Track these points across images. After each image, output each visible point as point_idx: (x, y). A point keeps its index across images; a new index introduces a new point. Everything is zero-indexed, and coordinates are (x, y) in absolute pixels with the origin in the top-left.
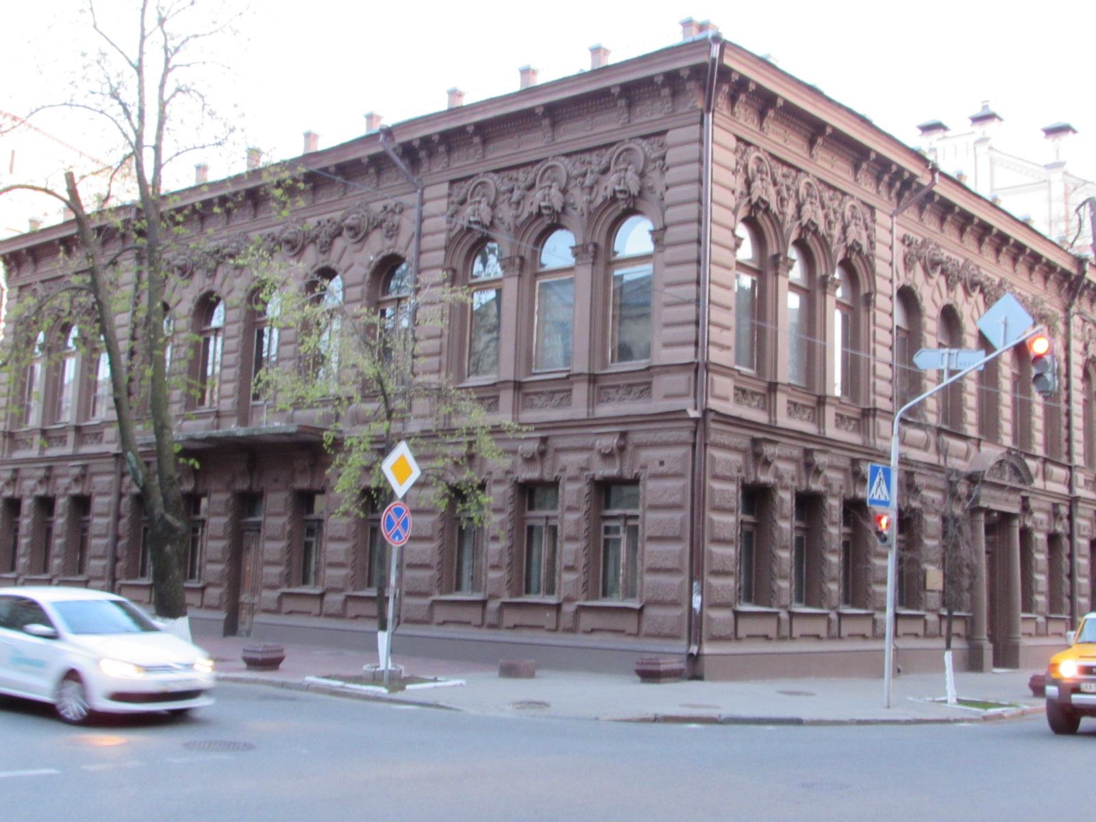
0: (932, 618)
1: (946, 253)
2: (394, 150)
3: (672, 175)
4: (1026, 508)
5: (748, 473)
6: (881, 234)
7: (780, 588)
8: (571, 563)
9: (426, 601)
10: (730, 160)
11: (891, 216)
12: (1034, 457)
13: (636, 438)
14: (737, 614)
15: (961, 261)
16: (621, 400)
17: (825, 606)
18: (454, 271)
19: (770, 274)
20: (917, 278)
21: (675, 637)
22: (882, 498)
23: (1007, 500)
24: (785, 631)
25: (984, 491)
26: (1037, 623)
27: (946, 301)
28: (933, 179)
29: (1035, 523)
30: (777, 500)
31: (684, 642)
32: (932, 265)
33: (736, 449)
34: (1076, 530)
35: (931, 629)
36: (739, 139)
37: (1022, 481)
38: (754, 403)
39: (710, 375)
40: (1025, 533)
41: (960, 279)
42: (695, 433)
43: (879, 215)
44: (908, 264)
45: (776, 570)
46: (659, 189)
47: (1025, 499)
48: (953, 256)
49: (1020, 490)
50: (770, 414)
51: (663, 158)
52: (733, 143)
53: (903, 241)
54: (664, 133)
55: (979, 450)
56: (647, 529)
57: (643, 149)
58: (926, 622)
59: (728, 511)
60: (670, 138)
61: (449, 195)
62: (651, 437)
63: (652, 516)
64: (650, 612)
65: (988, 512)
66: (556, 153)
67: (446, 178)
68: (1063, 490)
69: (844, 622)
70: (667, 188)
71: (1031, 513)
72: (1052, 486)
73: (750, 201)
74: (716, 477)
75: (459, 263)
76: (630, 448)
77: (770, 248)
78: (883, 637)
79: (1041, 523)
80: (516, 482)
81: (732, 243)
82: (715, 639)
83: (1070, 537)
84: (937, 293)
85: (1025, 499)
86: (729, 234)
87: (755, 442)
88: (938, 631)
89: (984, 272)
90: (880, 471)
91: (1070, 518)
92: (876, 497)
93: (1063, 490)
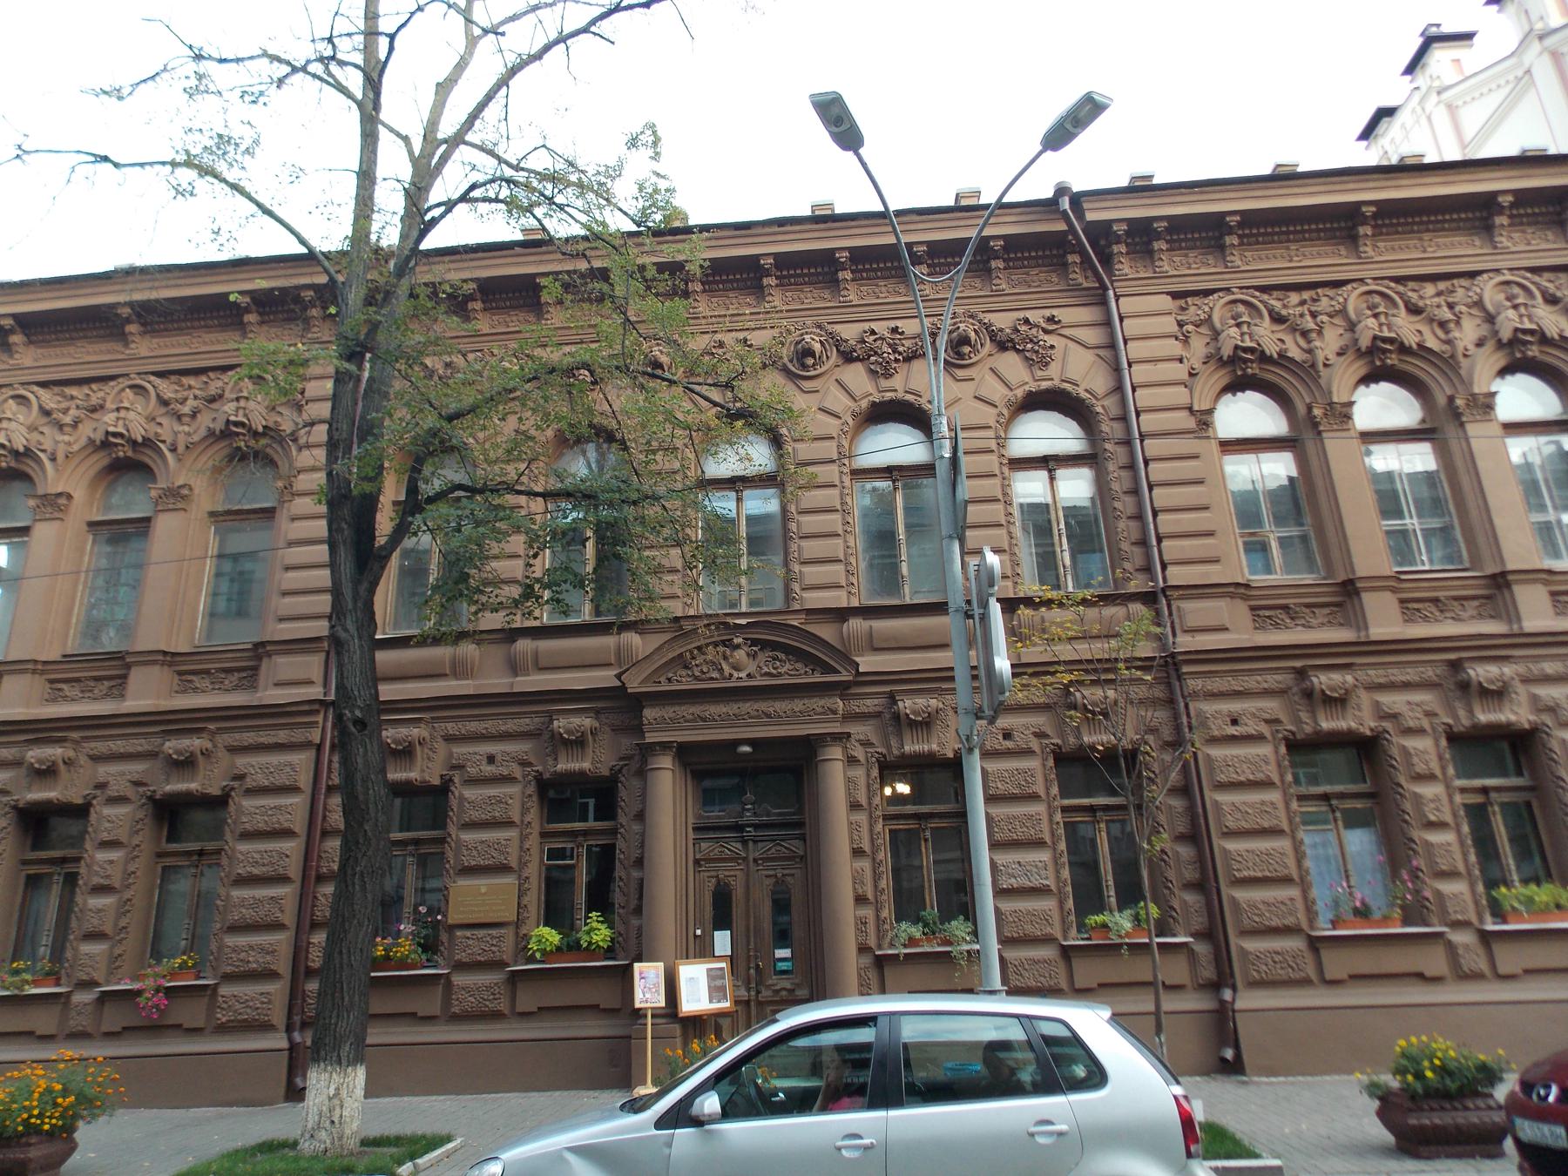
0: (1461, 938)
30: (1395, 752)
56: (87, 876)
65: (685, 753)
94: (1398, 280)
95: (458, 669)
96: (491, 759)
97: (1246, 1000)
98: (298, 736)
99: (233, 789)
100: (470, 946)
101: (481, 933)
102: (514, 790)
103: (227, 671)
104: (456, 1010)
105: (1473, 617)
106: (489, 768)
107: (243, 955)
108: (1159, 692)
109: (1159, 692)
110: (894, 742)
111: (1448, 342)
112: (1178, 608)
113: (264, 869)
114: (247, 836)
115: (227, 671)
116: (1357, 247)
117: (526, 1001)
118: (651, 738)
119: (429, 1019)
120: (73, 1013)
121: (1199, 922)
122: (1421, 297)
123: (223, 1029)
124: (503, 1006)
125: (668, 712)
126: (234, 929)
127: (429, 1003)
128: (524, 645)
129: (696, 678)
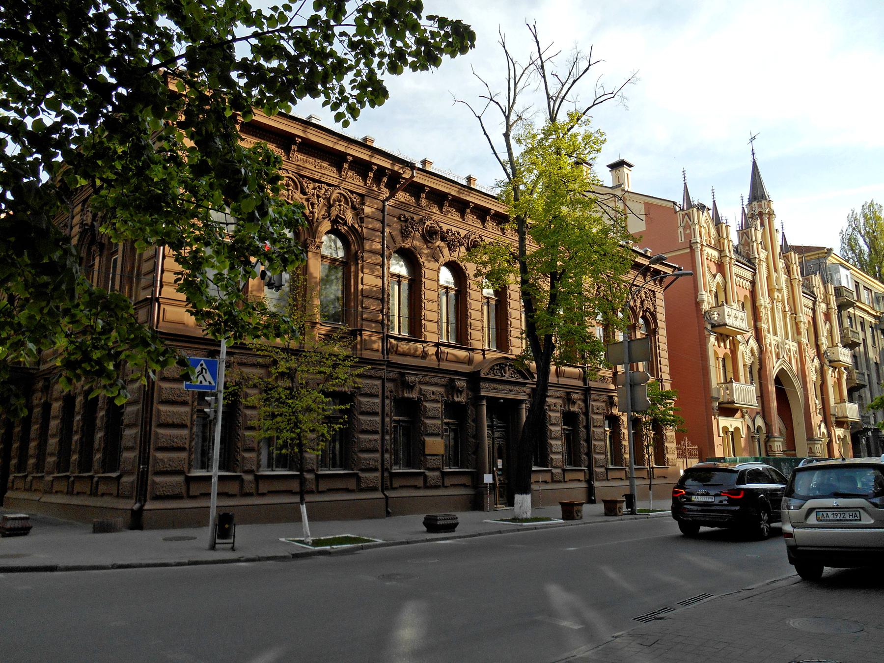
7: (244, 458)
14: (189, 480)
17: (238, 470)
21: (128, 497)
22: (204, 383)
26: (552, 473)
28: (413, 173)
31: (133, 501)
34: (590, 409)
35: (431, 482)
37: (525, 378)
45: (239, 445)
48: (454, 229)
49: (524, 384)
53: (399, 218)
58: (425, 477)
65: (490, 400)
67: (81, 200)
68: (580, 383)
82: (157, 498)
83: (586, 414)
88: (440, 483)
90: (202, 362)
91: (585, 401)
93: (580, 383)
96: (433, 393)
97: (597, 484)
98: (378, 374)
99: (355, 392)
100: (432, 462)
101: (434, 458)
102: (439, 405)
104: (428, 484)
106: (433, 396)
107: (368, 462)
108: (582, 397)
109: (582, 397)
113: (373, 428)
114: (363, 413)
117: (447, 482)
118: (483, 394)
119: (419, 488)
121: (586, 464)
123: (362, 490)
124: (440, 483)
125: (487, 385)
126: (362, 451)
127: (420, 482)
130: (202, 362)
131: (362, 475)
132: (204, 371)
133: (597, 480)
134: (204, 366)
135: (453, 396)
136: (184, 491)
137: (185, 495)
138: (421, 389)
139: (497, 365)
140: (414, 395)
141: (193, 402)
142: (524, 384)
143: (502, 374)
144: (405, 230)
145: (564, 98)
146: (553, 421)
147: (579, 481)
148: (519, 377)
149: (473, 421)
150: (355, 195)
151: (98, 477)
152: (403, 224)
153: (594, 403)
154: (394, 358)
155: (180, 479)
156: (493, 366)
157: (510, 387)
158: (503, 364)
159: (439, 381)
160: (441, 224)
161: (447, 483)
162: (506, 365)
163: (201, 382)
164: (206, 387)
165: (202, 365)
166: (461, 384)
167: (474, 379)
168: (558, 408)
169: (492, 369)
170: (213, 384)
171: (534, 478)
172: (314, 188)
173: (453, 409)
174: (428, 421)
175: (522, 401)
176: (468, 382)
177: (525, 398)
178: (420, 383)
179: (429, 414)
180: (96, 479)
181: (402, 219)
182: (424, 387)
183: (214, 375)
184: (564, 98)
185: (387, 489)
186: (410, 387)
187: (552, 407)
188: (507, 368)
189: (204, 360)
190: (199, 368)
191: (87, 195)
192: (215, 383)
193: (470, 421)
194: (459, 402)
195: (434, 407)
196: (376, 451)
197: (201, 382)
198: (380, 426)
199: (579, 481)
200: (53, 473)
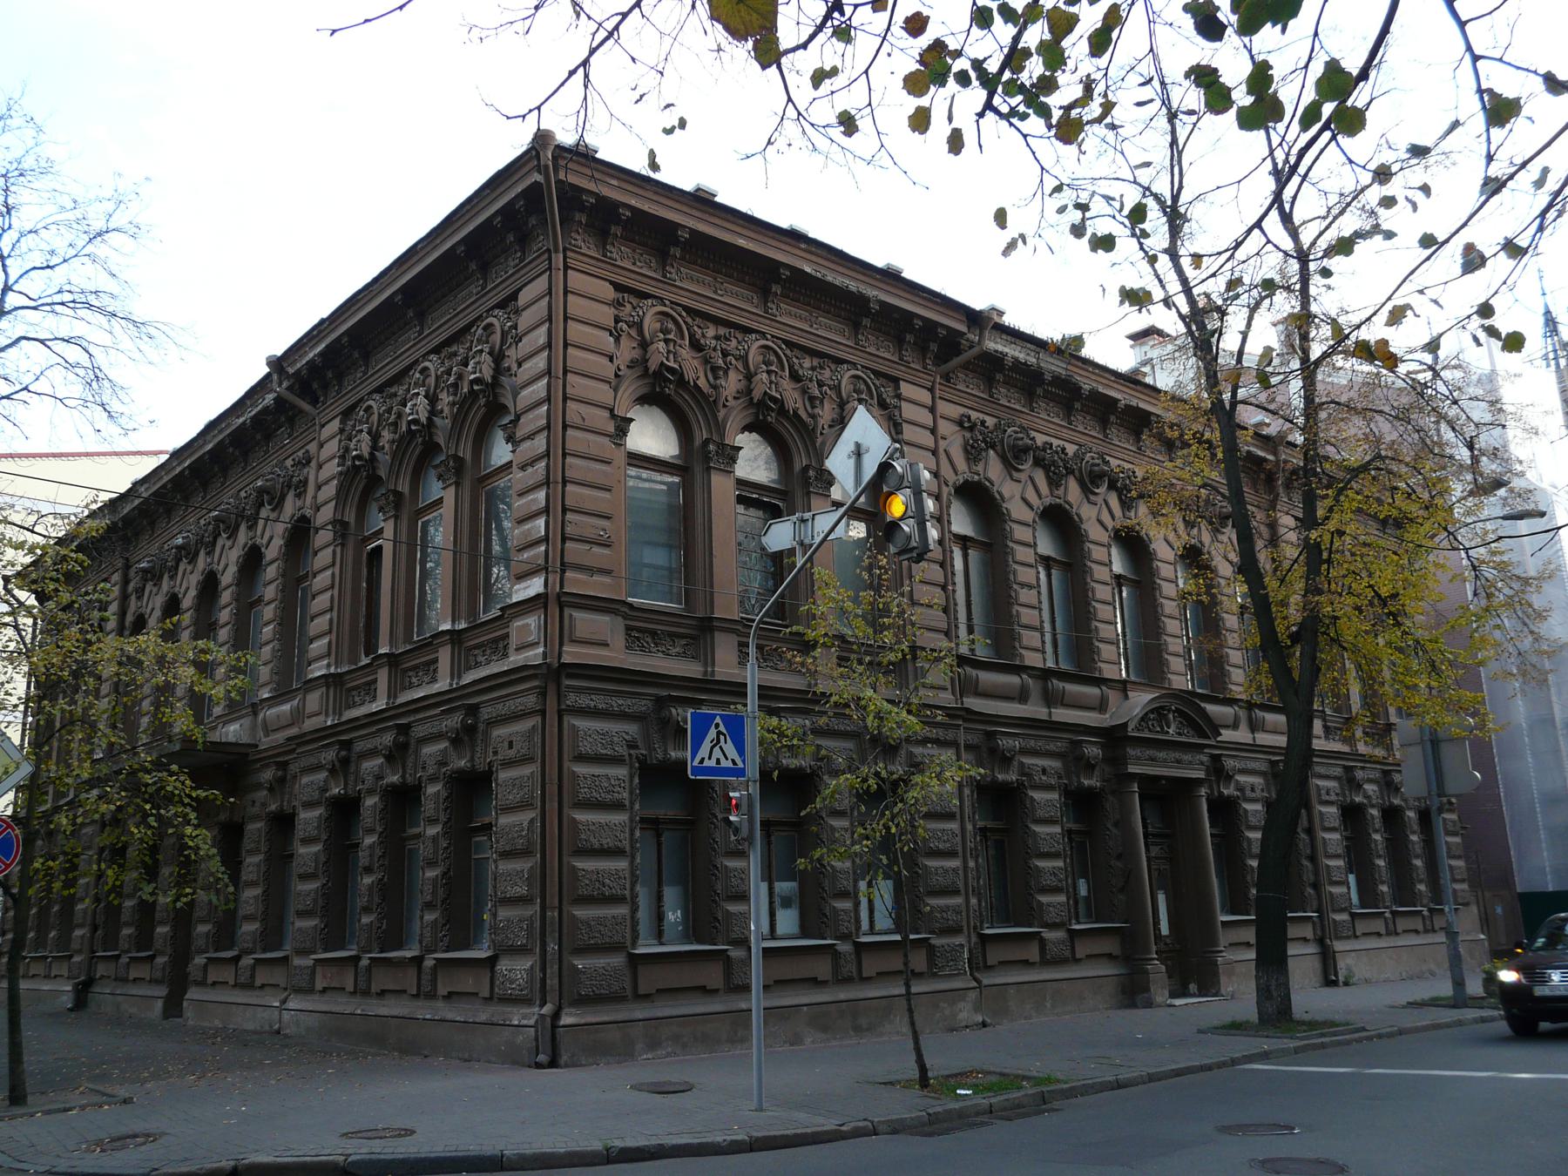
1: (1040, 439)
2: (289, 389)
3: (526, 345)
4: (1218, 771)
5: (651, 749)
6: (908, 411)
8: (429, 898)
9: (307, 962)
10: (606, 315)
11: (931, 390)
12: (1231, 702)
13: (486, 713)
14: (635, 961)
15: (1071, 449)
16: (488, 662)
18: (345, 525)
19: (698, 469)
20: (993, 469)
22: (725, 764)
23: (1178, 762)
24: (850, 968)
25: (1131, 752)
27: (1048, 501)
29: (1241, 789)
32: (1013, 457)
33: (622, 716)
36: (618, 287)
38: (674, 651)
39: (567, 611)
40: (1225, 810)
41: (1070, 472)
42: (543, 694)
43: (906, 389)
44: (973, 453)
45: (719, 888)
46: (514, 367)
47: (1216, 759)
48: (1055, 442)
50: (706, 665)
51: (515, 327)
52: (609, 293)
53: (960, 424)
54: (514, 296)
55: (1126, 697)
57: (497, 320)
58: (1043, 943)
59: (617, 806)
60: (524, 297)
61: (342, 431)
62: (503, 709)
63: (504, 820)
64: (503, 965)
65: (1144, 780)
66: (423, 351)
67: (339, 410)
69: (642, 970)
70: (520, 365)
71: (1229, 778)
72: (1263, 739)
73: (647, 369)
74: (581, 758)
75: (350, 517)
76: (481, 727)
77: (697, 433)
78: (746, 988)
79: (1253, 790)
80: (385, 790)
81: (611, 428)
84: (1030, 489)
85: (1216, 759)
86: (607, 414)
87: (661, 702)
88: (1068, 954)
89: (1114, 462)
90: (718, 720)
92: (707, 763)
94: (790, 344)
95: (1022, 696)
96: (1044, 771)
97: (1339, 946)
103: (672, 636)
105: (678, 655)
106: (1044, 778)
110: (1215, 787)
111: (715, 387)
112: (571, 615)
113: (948, 845)
115: (672, 636)
116: (856, 334)
118: (1132, 769)
120: (842, 962)
121: (1315, 904)
122: (703, 336)
127: (1033, 953)
128: (1057, 684)
129: (1150, 730)
130: (718, 720)
131: (937, 941)
132: (722, 737)
133: (1339, 938)
134: (722, 728)
135: (1078, 777)
136: (628, 985)
137: (629, 992)
138: (1022, 764)
139: (1152, 711)
140: (1012, 777)
141: (632, 803)
142: (1199, 748)
143: (1162, 728)
144: (972, 447)
145: (1306, 175)
146: (1253, 820)
147: (1305, 939)
148: (1192, 732)
149: (1116, 825)
150: (883, 381)
151: (370, 958)
152: (968, 435)
153: (1320, 783)
154: (974, 703)
155: (617, 960)
156: (1146, 714)
157: (1177, 755)
158: (1162, 708)
159: (1052, 747)
160: (1033, 434)
161: (1081, 952)
162: (1169, 711)
163: (718, 761)
164: (727, 771)
165: (717, 726)
166: (1093, 751)
167: (1114, 737)
168: (1258, 794)
169: (1144, 718)
170: (741, 765)
171: (1224, 938)
172: (813, 369)
173: (1082, 803)
174: (1038, 829)
175: (1197, 782)
176: (1103, 746)
177: (1201, 775)
178: (1025, 751)
179: (1040, 813)
180: (364, 962)
181: (966, 425)
182: (1027, 761)
183: (741, 750)
184: (1306, 175)
185: (978, 969)
186: (1005, 760)
187: (1249, 794)
188: (1171, 716)
189: (721, 716)
190: (712, 733)
191: (358, 397)
192: (744, 762)
193: (1109, 826)
194: (1090, 788)
195: (1045, 799)
196: (956, 892)
197: (718, 761)
198: (959, 839)
199: (1305, 939)
200: (314, 953)
